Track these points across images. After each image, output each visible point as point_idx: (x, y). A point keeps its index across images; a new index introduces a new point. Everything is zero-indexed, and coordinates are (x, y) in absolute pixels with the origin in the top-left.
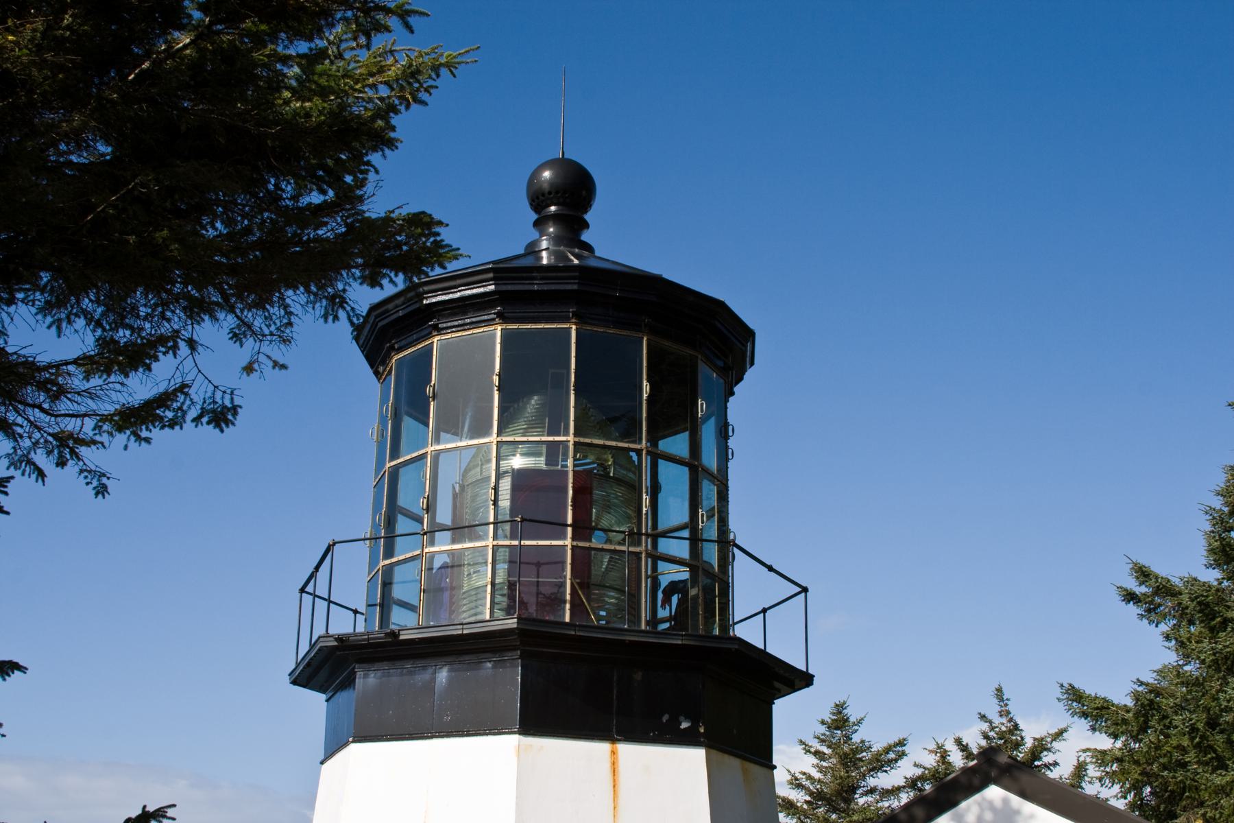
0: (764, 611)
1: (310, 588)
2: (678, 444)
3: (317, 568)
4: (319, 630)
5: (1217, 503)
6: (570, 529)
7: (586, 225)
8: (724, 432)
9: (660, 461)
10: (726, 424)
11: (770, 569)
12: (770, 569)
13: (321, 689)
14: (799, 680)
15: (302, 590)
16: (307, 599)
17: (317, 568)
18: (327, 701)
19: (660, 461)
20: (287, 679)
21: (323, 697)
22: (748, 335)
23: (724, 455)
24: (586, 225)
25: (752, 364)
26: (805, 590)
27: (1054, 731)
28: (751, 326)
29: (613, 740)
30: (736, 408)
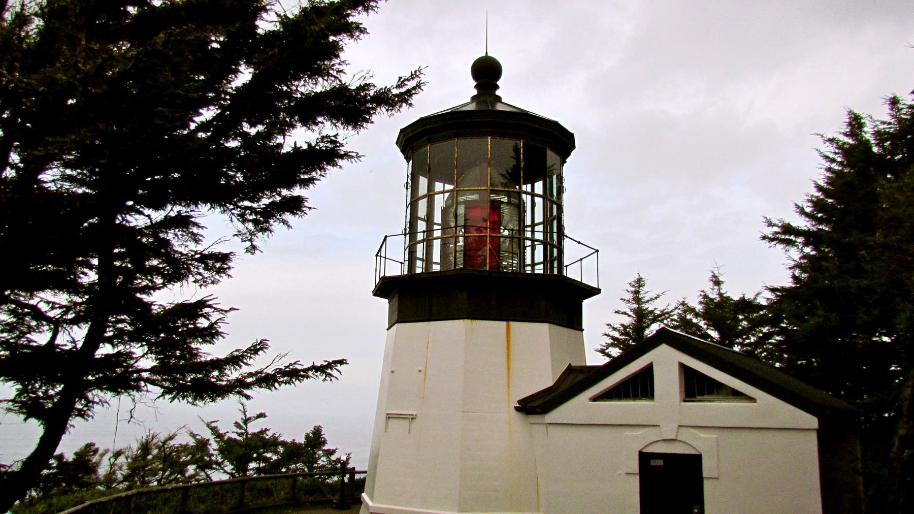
3: (381, 247)
4: (382, 275)
5: (270, 433)
7: (498, 87)
8: (560, 179)
10: (562, 177)
14: (595, 291)
15: (377, 255)
17: (381, 247)
22: (571, 136)
23: (560, 190)
24: (498, 87)
26: (597, 251)
28: (571, 131)
30: (566, 169)
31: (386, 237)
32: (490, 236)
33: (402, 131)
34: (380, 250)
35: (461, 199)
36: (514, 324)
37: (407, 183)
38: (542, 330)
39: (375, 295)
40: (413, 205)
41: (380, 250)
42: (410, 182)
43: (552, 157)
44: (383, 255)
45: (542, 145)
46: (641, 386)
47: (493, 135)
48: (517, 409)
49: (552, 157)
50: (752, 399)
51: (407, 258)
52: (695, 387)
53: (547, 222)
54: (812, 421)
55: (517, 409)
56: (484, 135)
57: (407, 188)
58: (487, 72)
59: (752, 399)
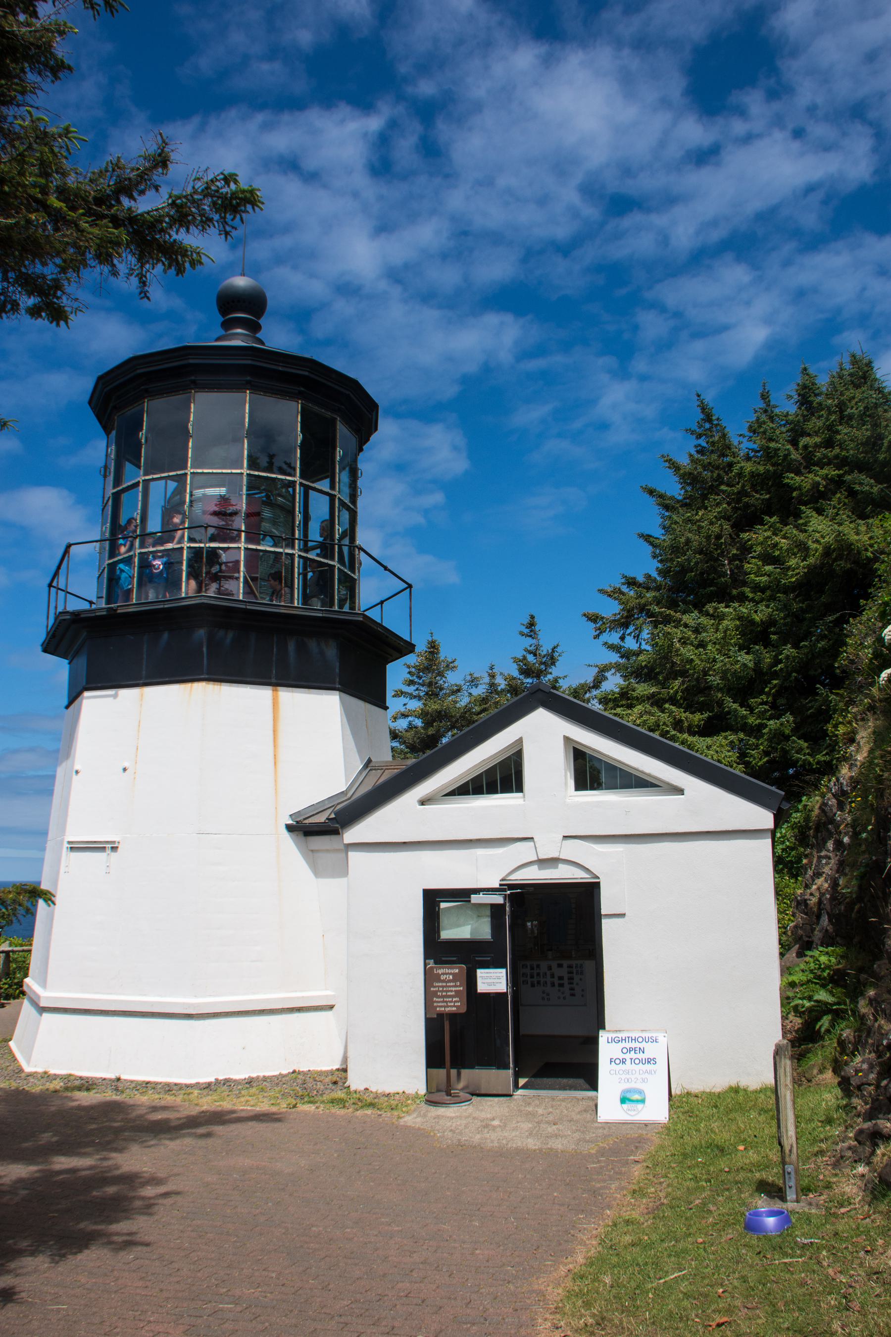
0: (382, 603)
1: (54, 584)
2: (324, 485)
3: (59, 567)
4: (60, 609)
6: (243, 534)
8: (354, 474)
9: (311, 492)
13: (63, 656)
17: (59, 567)
19: (311, 492)
20: (40, 649)
25: (376, 429)
26: (410, 586)
27: (670, 472)
31: (69, 546)
37: (106, 467)
46: (506, 777)
47: (255, 388)
48: (290, 828)
50: (681, 791)
51: (104, 594)
52: (589, 773)
54: (764, 818)
55: (290, 828)
56: (238, 387)
57: (105, 476)
59: (681, 791)
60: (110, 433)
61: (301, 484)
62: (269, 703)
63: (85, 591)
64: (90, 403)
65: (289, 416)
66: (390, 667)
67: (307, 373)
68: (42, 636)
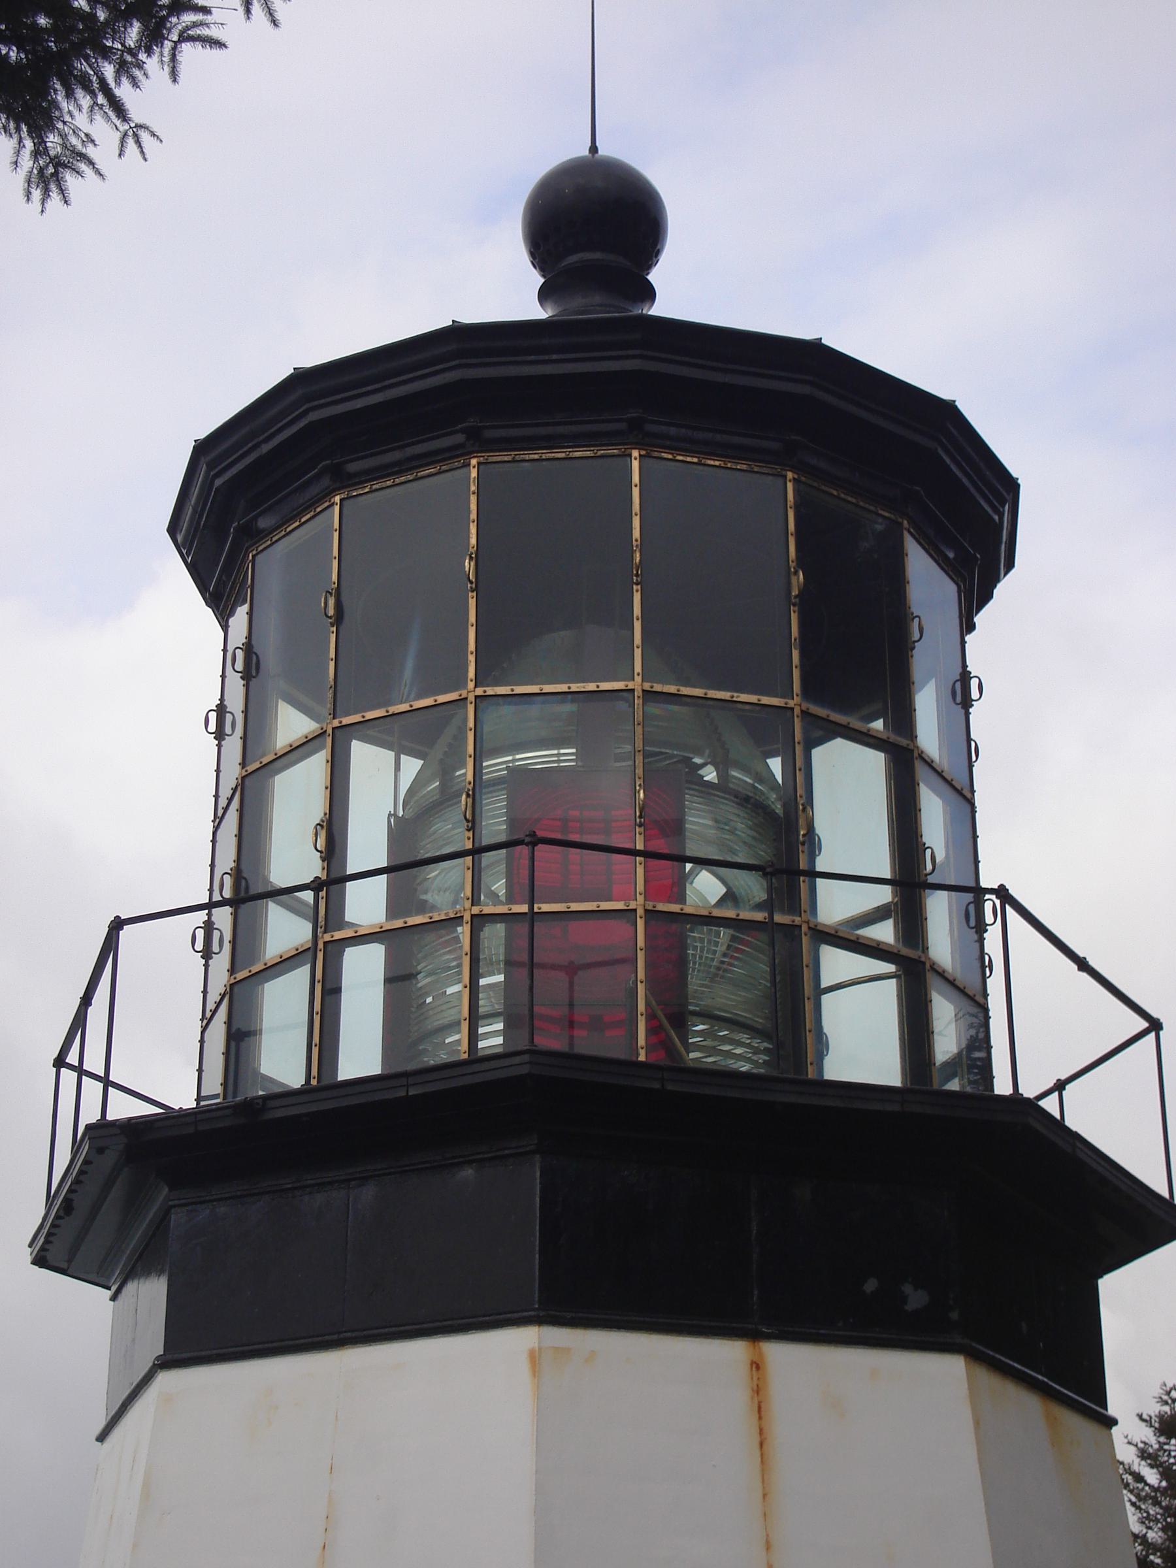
1: (72, 1058)
3: (86, 1000)
4: (91, 1115)
8: (962, 692)
10: (965, 677)
11: (1083, 965)
12: (1083, 965)
15: (60, 1062)
16: (69, 1077)
17: (86, 1000)
18: (114, 1298)
20: (27, 1255)
21: (108, 1293)
25: (1010, 565)
26: (1155, 1025)
29: (754, 1335)
31: (117, 925)
32: (651, 915)
33: (202, 448)
34: (79, 1022)
35: (496, 765)
36: (782, 1356)
37: (221, 710)
38: (936, 1384)
39: (40, 1261)
40: (245, 804)
41: (79, 1022)
42: (236, 705)
43: (926, 582)
44: (94, 1063)
45: (871, 507)
49: (926, 582)
53: (910, 879)
58: (596, 224)
60: (232, 613)
61: (805, 714)
62: (739, 1397)
63: (164, 1068)
64: (172, 530)
65: (764, 506)
66: (1100, 1281)
67: (806, 390)
68: (31, 1212)
